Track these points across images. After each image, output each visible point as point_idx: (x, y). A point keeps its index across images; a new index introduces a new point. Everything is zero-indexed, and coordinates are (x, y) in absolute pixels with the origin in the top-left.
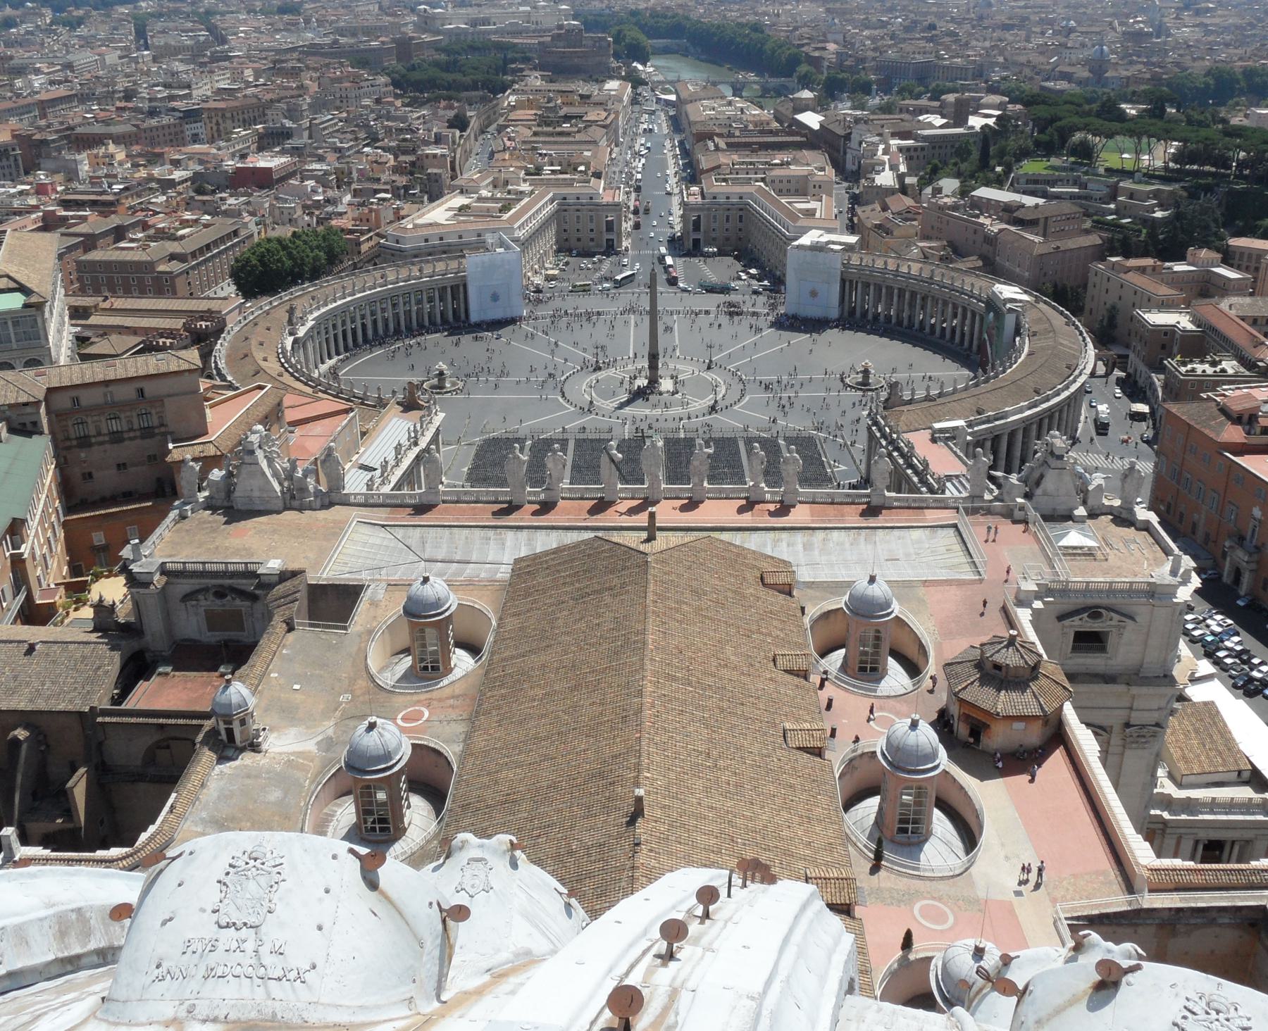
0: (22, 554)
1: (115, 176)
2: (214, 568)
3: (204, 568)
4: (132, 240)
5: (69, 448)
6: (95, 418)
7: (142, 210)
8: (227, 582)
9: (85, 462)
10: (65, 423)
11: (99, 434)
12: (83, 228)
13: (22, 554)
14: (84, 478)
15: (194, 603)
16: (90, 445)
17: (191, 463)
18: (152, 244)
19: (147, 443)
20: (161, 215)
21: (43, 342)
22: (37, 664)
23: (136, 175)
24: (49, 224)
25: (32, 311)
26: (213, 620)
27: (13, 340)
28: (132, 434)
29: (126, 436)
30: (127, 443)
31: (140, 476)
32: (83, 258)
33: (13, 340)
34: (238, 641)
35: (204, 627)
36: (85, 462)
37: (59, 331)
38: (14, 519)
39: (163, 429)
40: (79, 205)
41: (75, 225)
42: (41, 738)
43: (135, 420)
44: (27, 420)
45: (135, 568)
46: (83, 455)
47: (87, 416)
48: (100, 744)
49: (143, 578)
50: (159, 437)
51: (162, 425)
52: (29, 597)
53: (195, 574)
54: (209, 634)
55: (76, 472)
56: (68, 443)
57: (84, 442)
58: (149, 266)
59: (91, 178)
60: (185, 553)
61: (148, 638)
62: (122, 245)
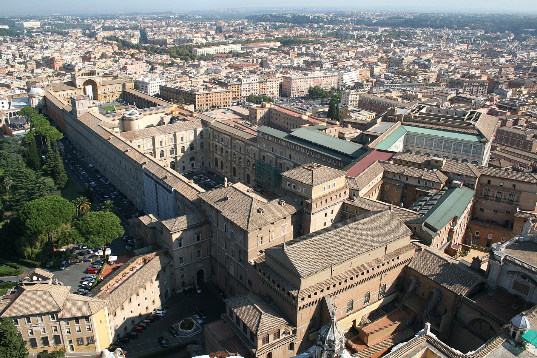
0: (454, 229)
1: (520, 100)
2: (526, 266)
3: (522, 264)
4: (521, 126)
5: (480, 198)
6: (493, 190)
7: (527, 115)
8: (529, 274)
9: (483, 204)
10: (482, 188)
11: (493, 197)
12: (503, 117)
13: (454, 229)
14: (481, 210)
15: (512, 275)
16: (488, 199)
17: (531, 222)
18: (528, 129)
19: (509, 206)
20: (535, 119)
21: (481, 156)
22: (448, 270)
23: (529, 101)
24: (491, 112)
25: (482, 144)
26: (516, 285)
27: (472, 152)
28: (504, 201)
29: (502, 200)
30: (501, 203)
31: (500, 217)
32: (502, 128)
33: (472, 152)
34: (523, 298)
35: (511, 286)
36: (483, 204)
37: (487, 153)
38: (456, 216)
39: (517, 203)
40: (505, 108)
41: (501, 115)
42: (440, 296)
43: (496, 194)
44: (471, 183)
45: (496, 252)
46: (484, 202)
47: (503, 191)
48: (458, 308)
49: (497, 257)
50: (513, 205)
51: (517, 201)
52: (450, 244)
53: (517, 265)
54: (512, 289)
55: (479, 207)
56: (480, 196)
57: (486, 197)
58: (524, 137)
59: (511, 99)
60: (516, 255)
61: (489, 279)
62: (516, 127)
